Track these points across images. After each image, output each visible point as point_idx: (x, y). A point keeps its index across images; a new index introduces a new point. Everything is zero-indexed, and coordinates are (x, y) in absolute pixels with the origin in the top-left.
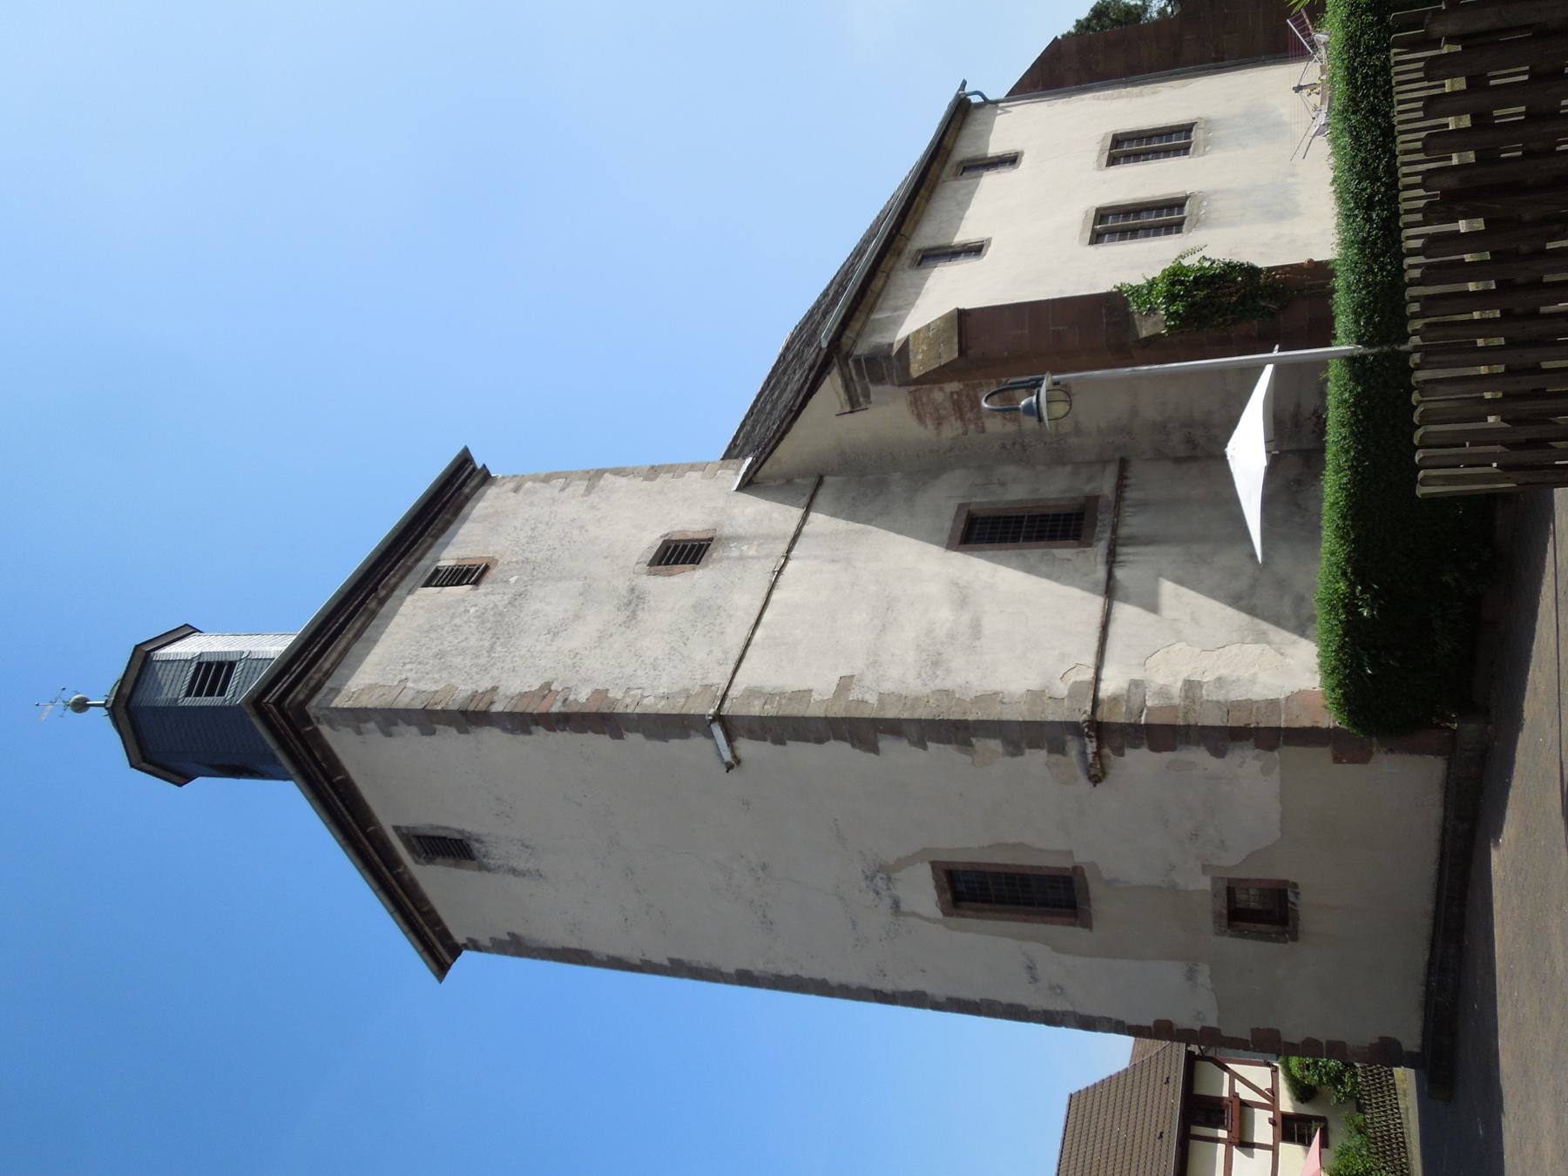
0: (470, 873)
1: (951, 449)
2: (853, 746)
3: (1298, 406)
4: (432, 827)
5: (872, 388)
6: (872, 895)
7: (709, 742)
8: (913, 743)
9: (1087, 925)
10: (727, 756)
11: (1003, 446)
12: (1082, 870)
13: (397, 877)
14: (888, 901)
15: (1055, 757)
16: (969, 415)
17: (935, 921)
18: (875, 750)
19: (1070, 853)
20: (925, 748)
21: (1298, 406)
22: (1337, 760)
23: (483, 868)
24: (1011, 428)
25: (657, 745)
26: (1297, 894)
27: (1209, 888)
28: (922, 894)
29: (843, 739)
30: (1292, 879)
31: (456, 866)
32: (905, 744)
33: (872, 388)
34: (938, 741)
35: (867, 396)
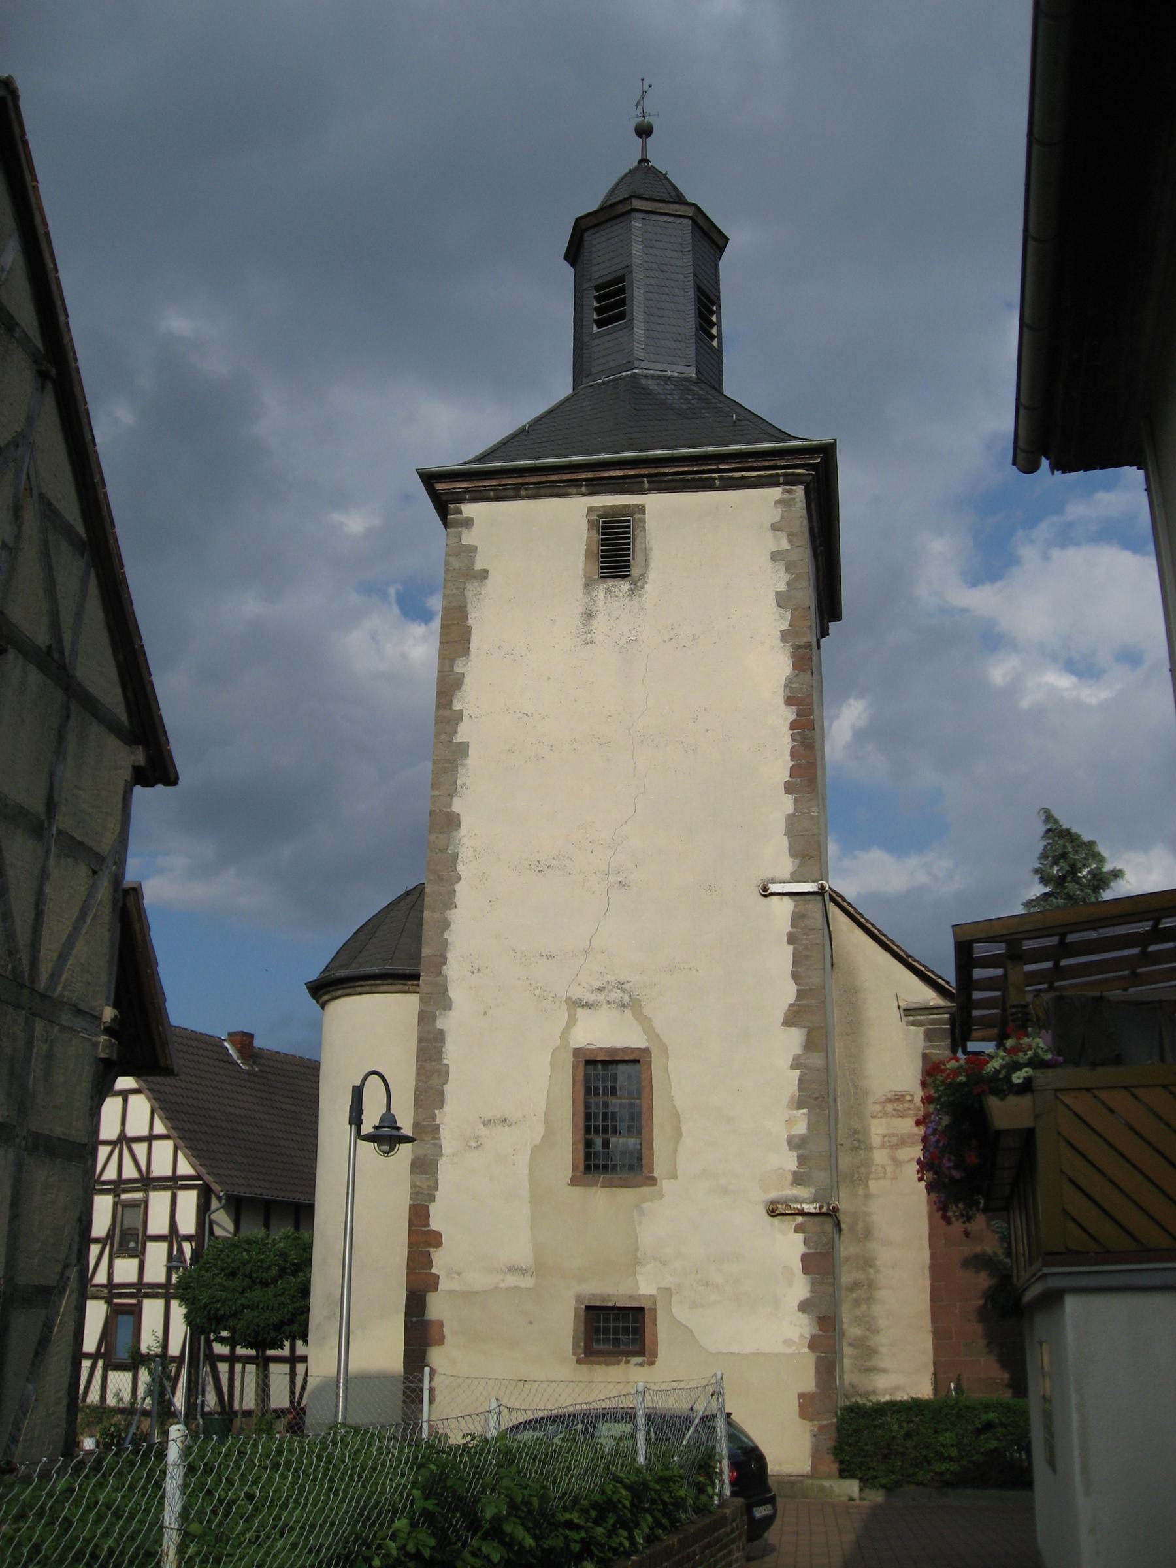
0: (581, 565)
1: (856, 1087)
2: (791, 1005)
3: (884, 1371)
4: (646, 552)
5: (921, 1029)
6: (598, 984)
7: (787, 876)
8: (797, 1058)
9: (574, 1182)
10: (774, 888)
11: (856, 1132)
12: (655, 1185)
13: (576, 483)
14: (591, 998)
15: (790, 1178)
16: (889, 1107)
17: (565, 1033)
18: (789, 1022)
19: (674, 1177)
20: (794, 1066)
21: (884, 1371)
22: (801, 1396)
23: (1049, 817)
24: (876, 1140)
25: (782, 826)
26: (641, 1365)
27: (641, 1292)
28: (604, 1032)
29: (798, 998)
30: (658, 1361)
31: (589, 553)
32: (798, 1051)
33: (921, 1029)
34: (801, 1080)
35: (913, 1024)
